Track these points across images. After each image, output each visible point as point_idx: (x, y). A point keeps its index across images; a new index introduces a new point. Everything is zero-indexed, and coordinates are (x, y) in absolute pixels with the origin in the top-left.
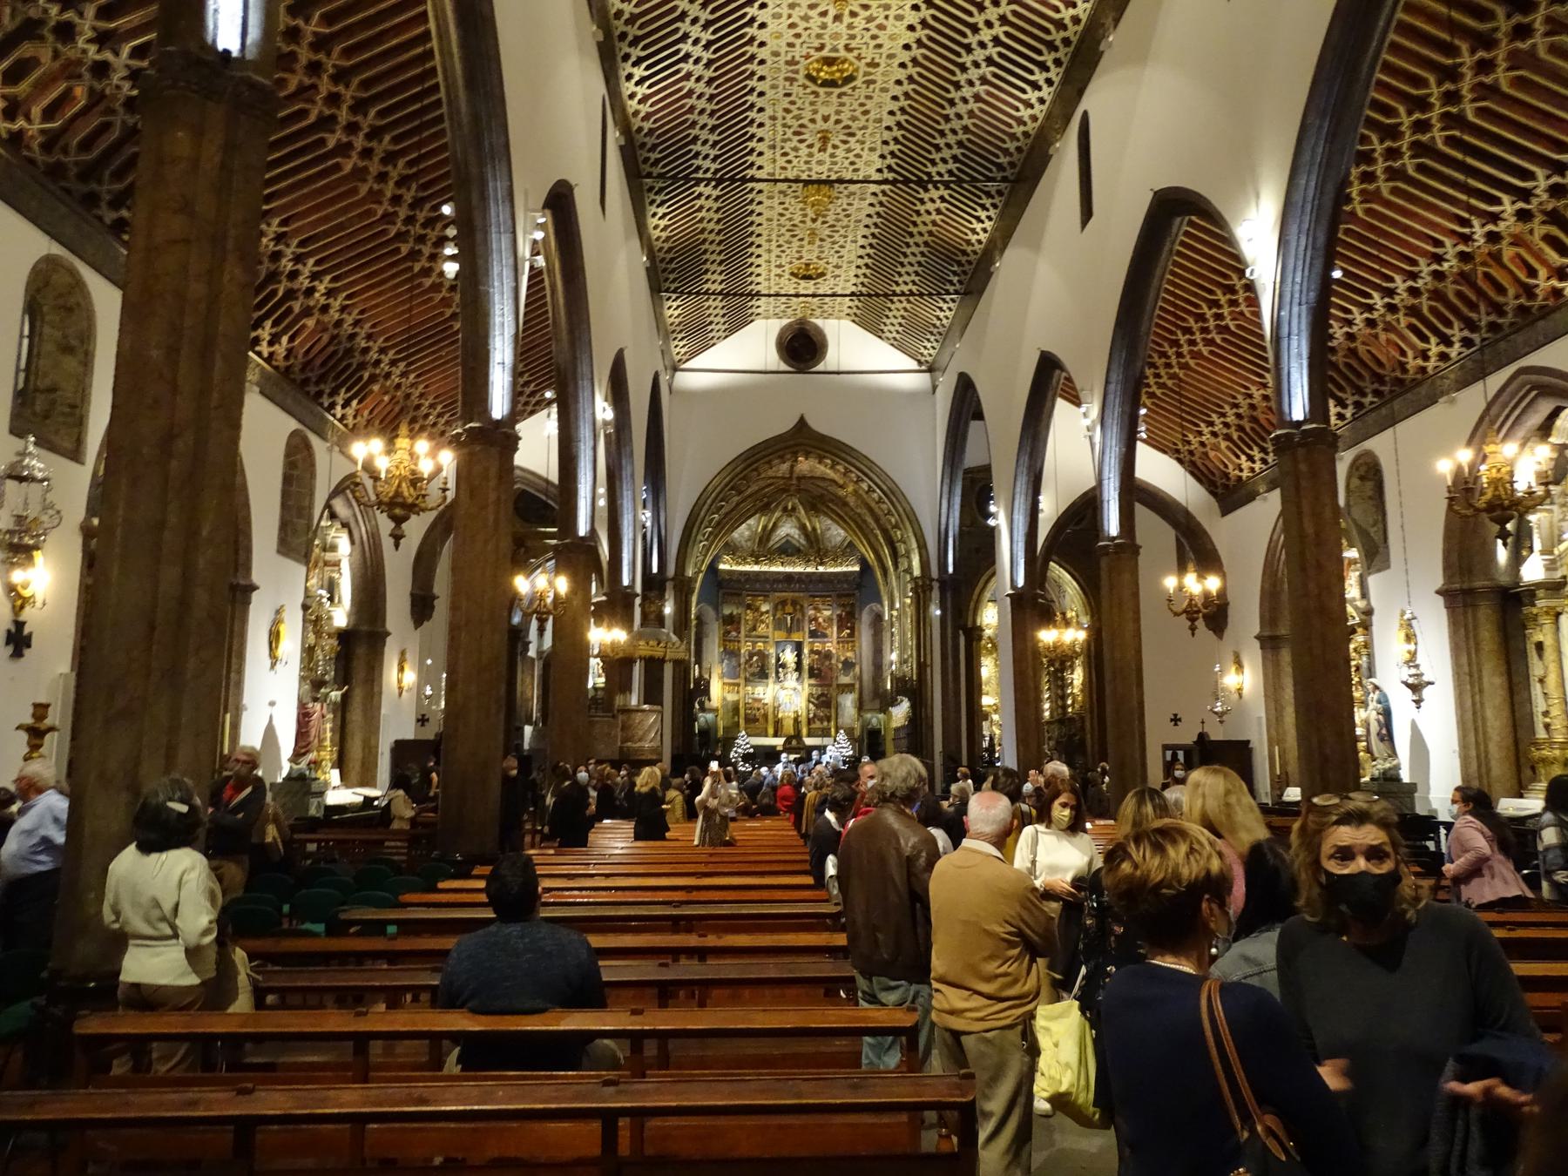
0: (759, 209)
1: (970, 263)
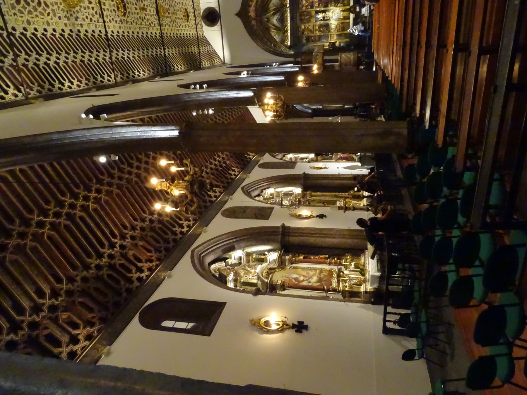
0: (169, 34)
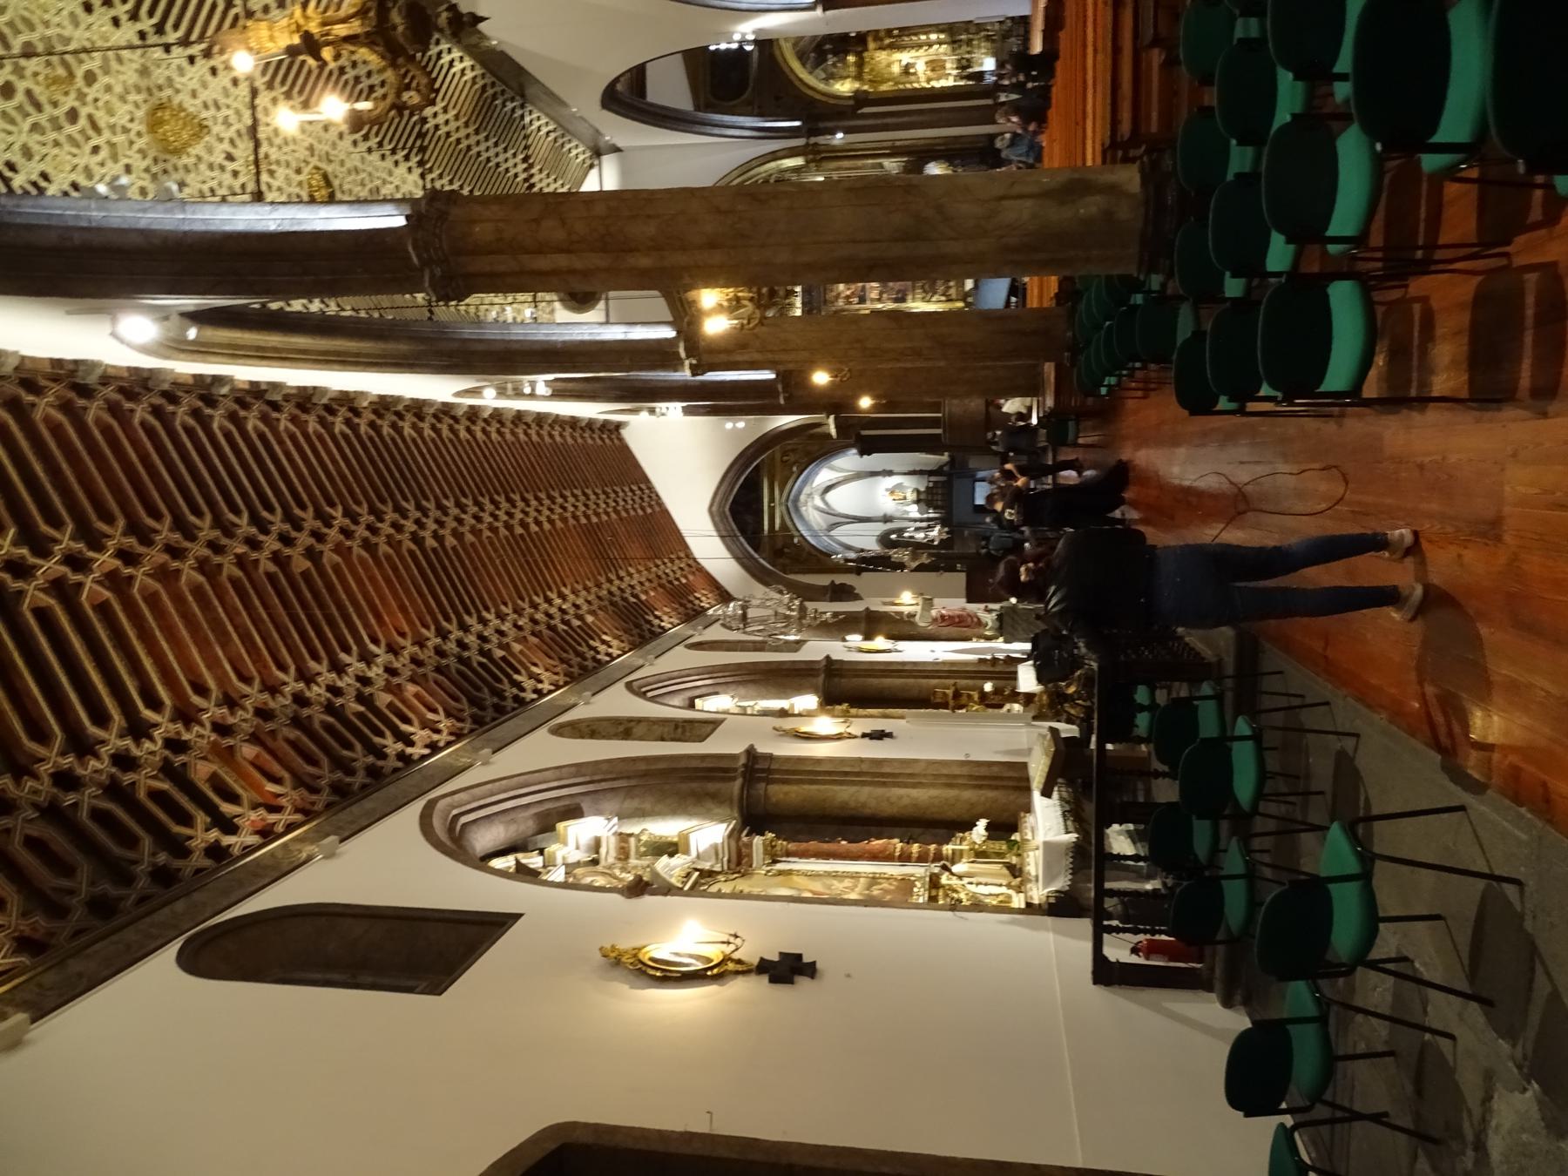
1: (493, 84)
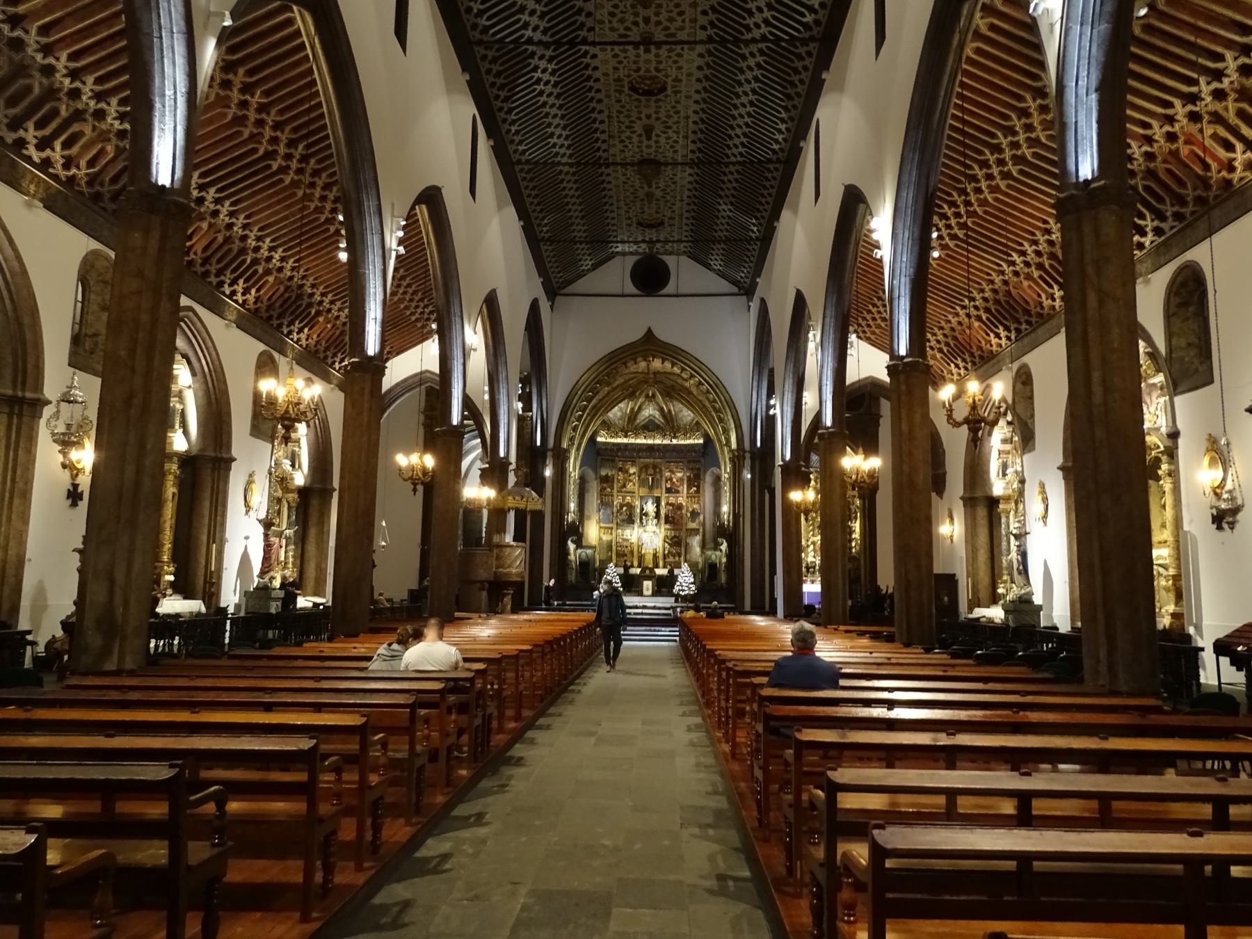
0: (608, 179)
